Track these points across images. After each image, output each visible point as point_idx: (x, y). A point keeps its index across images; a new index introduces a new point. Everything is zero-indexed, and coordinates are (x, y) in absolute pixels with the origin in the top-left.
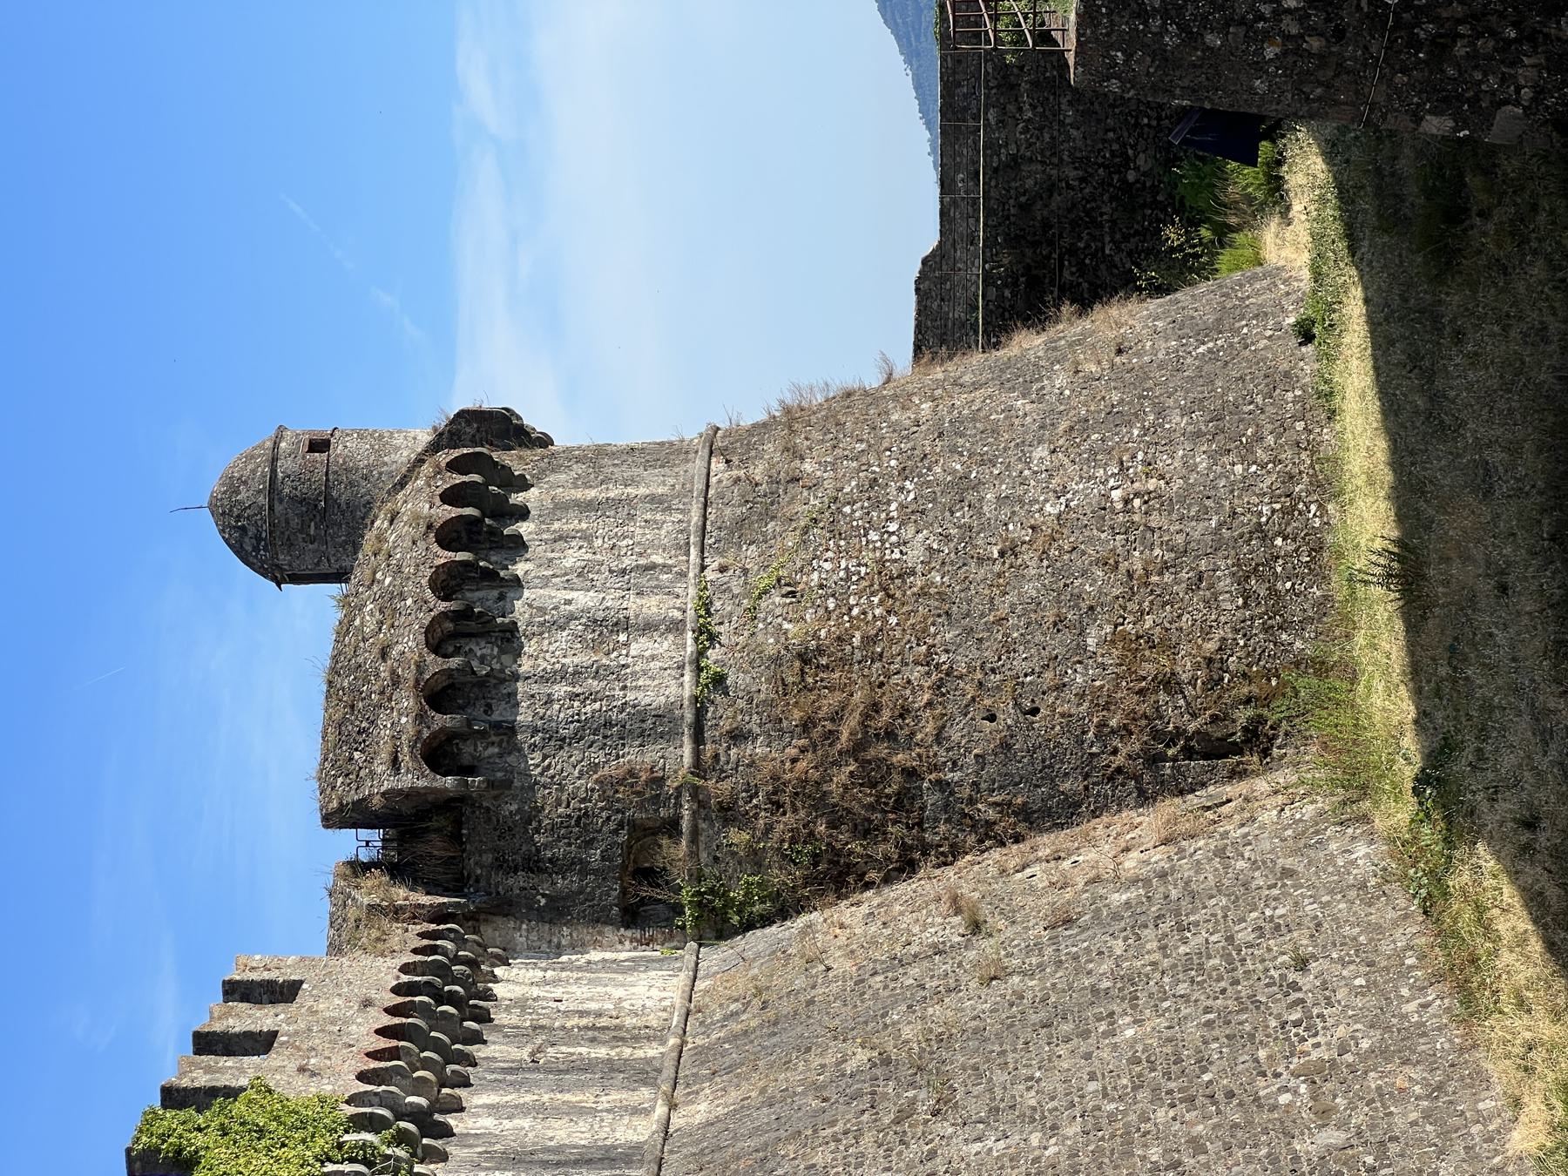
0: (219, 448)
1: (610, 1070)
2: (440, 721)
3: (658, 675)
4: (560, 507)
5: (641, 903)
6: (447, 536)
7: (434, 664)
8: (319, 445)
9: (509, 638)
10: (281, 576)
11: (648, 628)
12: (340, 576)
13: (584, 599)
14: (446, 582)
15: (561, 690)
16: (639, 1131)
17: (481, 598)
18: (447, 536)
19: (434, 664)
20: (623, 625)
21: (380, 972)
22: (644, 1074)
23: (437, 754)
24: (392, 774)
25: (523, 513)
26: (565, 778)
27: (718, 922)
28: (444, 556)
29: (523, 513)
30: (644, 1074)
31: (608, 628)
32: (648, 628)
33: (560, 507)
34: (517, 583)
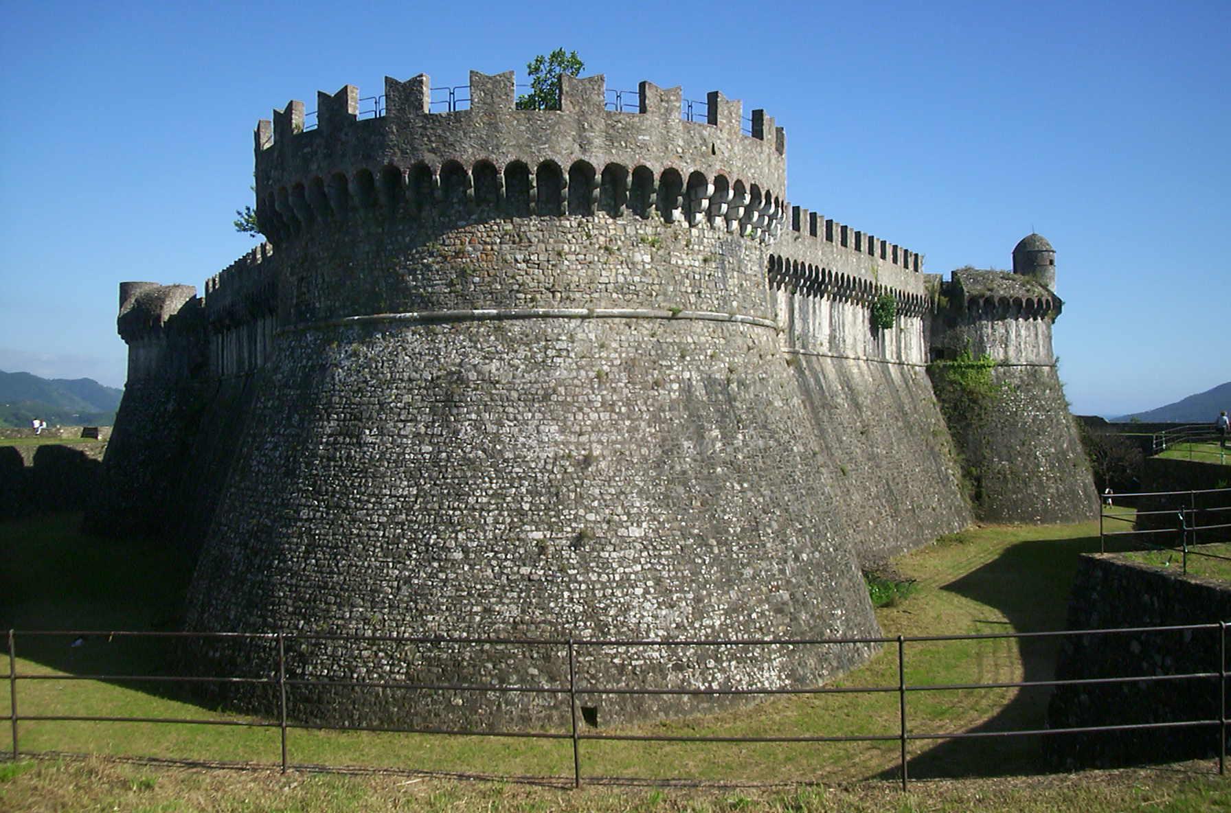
0: (1051, 236)
1: (899, 348)
2: (981, 302)
3: (995, 353)
4: (1035, 327)
5: (937, 352)
6: (1029, 301)
7: (996, 300)
8: (1051, 262)
9: (1003, 318)
10: (1016, 253)
11: (1006, 352)
12: (1015, 272)
13: (1013, 336)
14: (1018, 301)
15: (990, 331)
16: (888, 357)
17: (1013, 310)
18: (1029, 301)
19: (996, 300)
20: (1006, 346)
21: (921, 292)
22: (899, 357)
23: (973, 300)
24: (968, 289)
25: (1035, 319)
26: (967, 335)
27: (929, 371)
28: (1024, 301)
29: (1035, 319)
30: (899, 357)
31: (1005, 343)
32: (1006, 352)
33: (1035, 327)
34: (1017, 319)
